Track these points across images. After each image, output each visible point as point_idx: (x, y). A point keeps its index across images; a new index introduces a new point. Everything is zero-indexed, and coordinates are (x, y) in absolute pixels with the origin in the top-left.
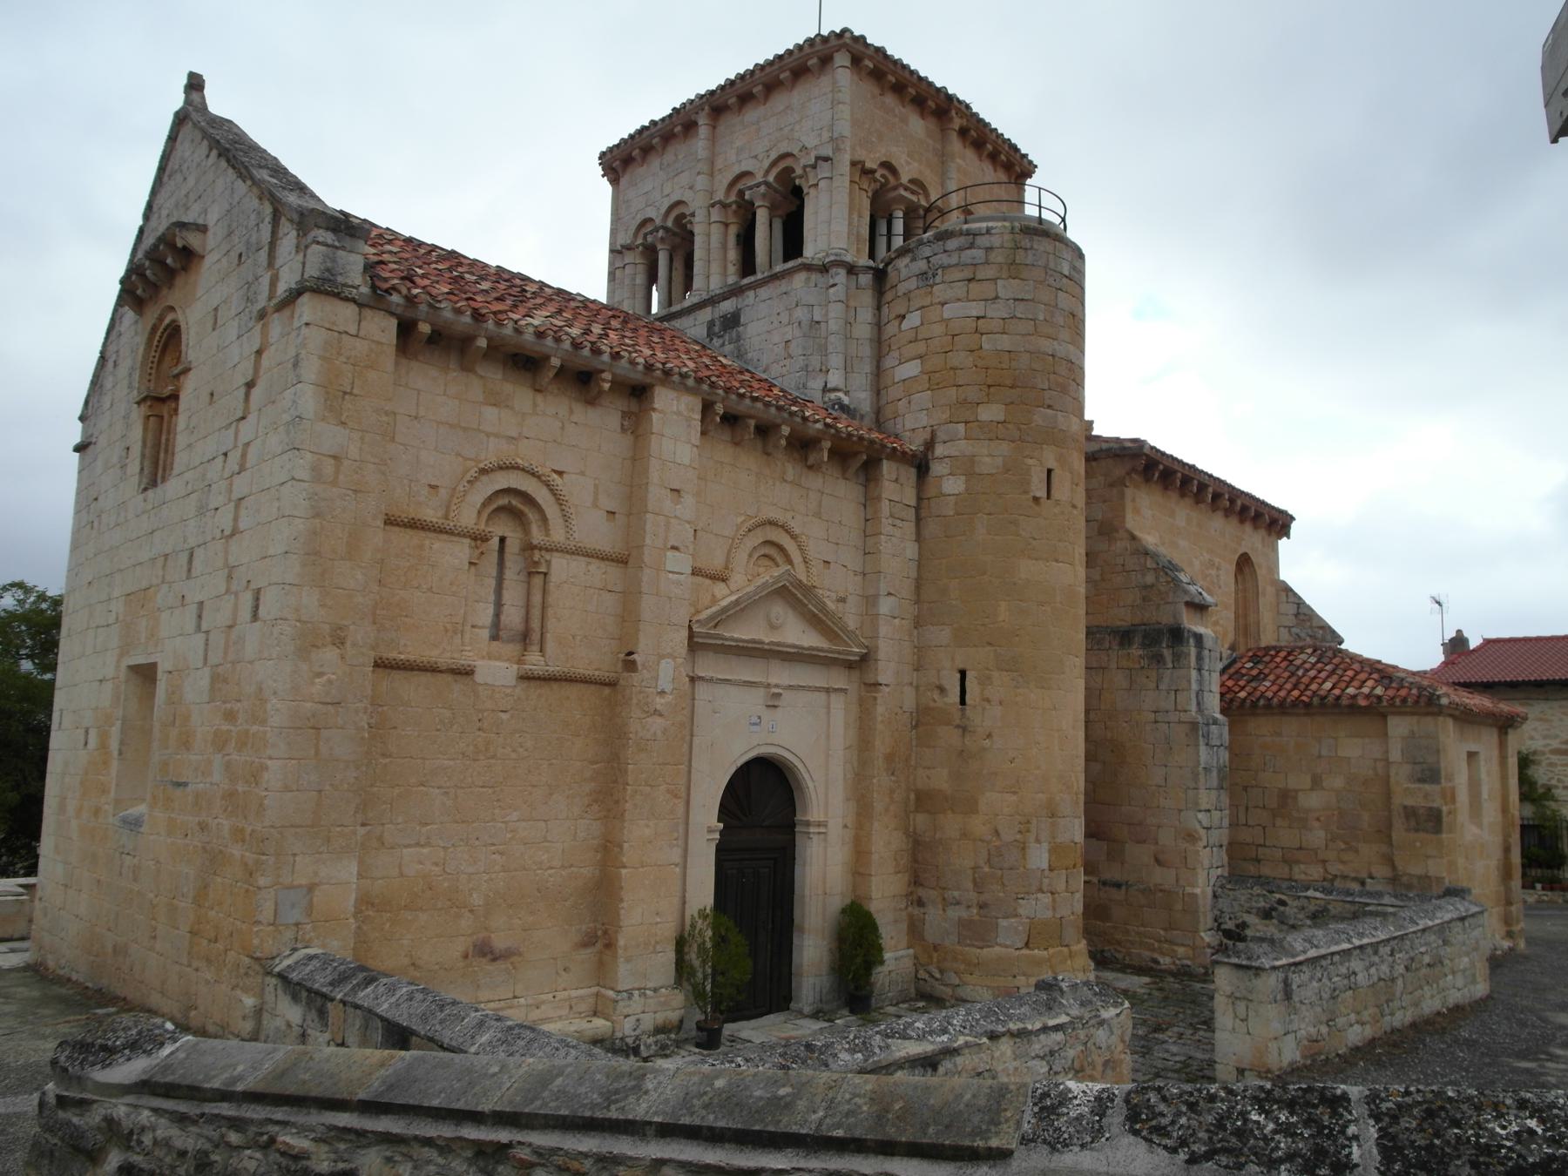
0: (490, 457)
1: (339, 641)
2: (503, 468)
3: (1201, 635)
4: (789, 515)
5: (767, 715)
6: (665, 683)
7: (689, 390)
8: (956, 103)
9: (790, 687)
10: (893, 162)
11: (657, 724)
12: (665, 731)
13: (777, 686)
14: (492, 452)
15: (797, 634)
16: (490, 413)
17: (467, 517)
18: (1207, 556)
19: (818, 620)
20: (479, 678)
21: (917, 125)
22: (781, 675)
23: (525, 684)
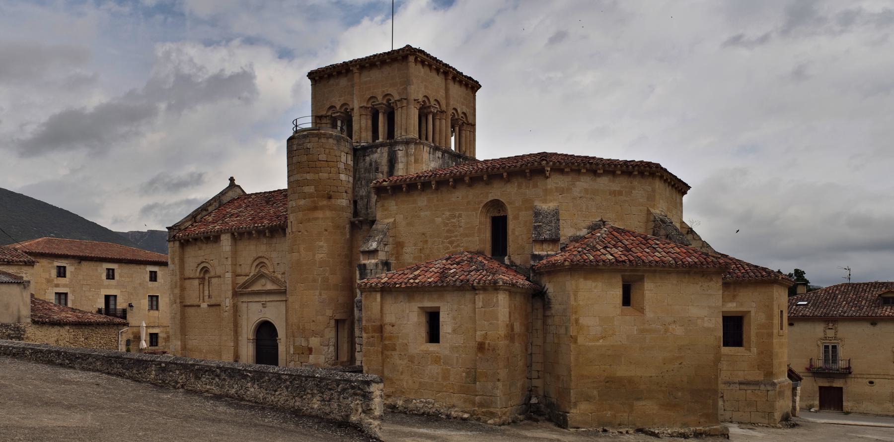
0: (200, 262)
1: (175, 303)
2: (199, 265)
3: (365, 265)
4: (266, 253)
5: (263, 309)
6: (227, 304)
7: (227, 233)
8: (349, 64)
9: (269, 301)
10: (333, 105)
11: (226, 314)
12: (228, 315)
13: (263, 301)
14: (201, 259)
15: (270, 286)
16: (199, 252)
17: (198, 275)
18: (448, 214)
19: (274, 281)
20: (201, 306)
21: (343, 82)
22: (264, 299)
23: (211, 308)
